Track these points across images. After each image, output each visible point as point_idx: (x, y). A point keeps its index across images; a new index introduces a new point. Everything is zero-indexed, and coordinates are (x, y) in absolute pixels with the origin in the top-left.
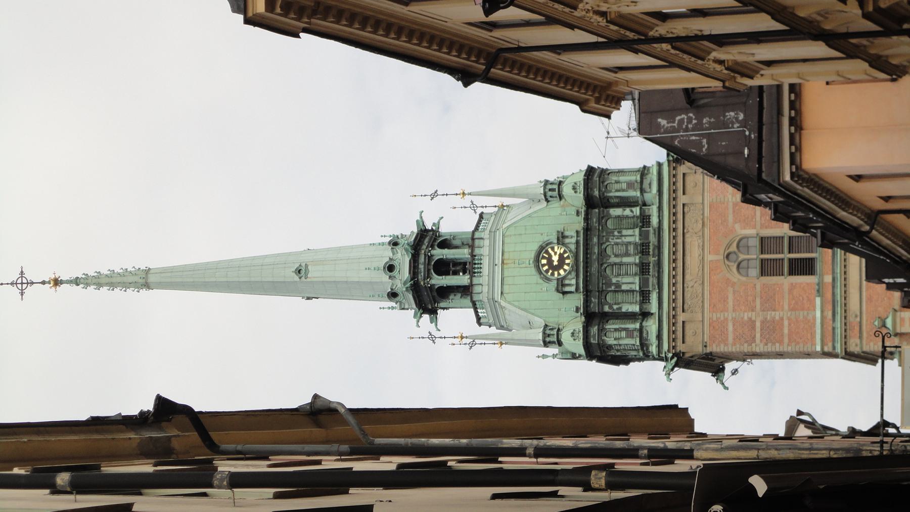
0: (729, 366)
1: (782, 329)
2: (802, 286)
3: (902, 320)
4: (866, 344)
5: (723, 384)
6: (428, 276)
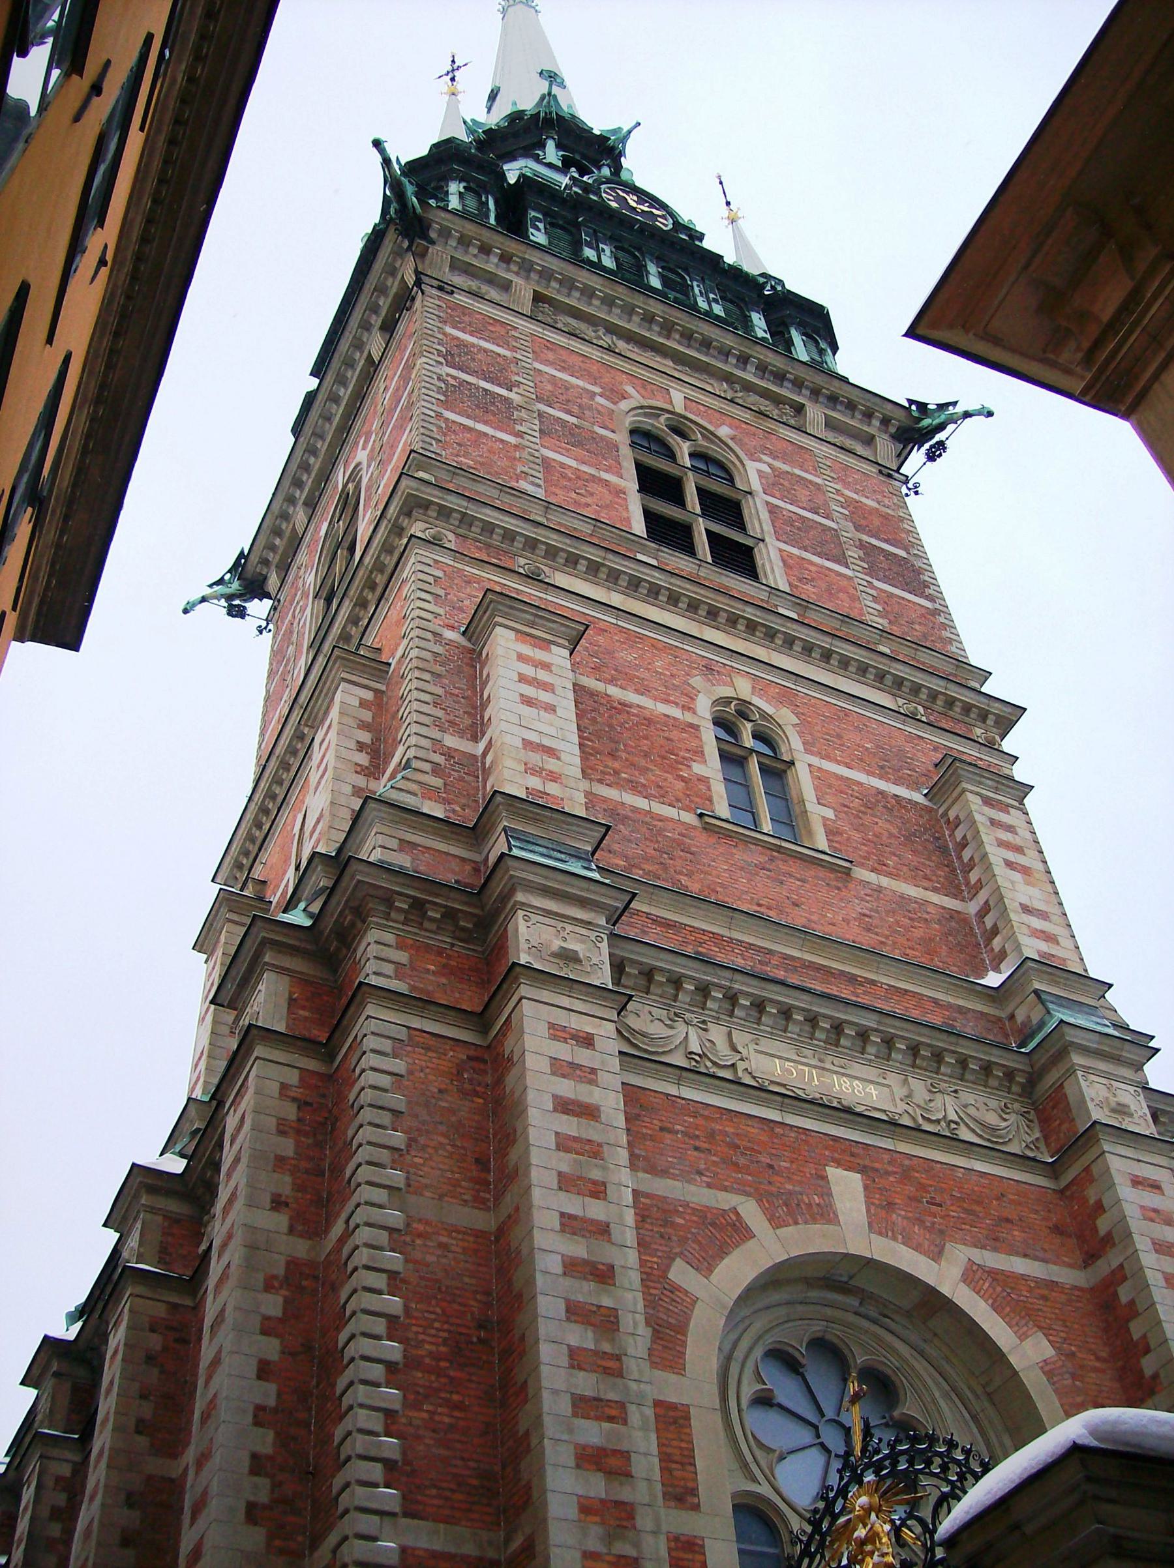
0: (259, 608)
1: (486, 423)
2: (620, 509)
3: (545, 644)
4: (436, 561)
5: (204, 600)
6: (559, 146)
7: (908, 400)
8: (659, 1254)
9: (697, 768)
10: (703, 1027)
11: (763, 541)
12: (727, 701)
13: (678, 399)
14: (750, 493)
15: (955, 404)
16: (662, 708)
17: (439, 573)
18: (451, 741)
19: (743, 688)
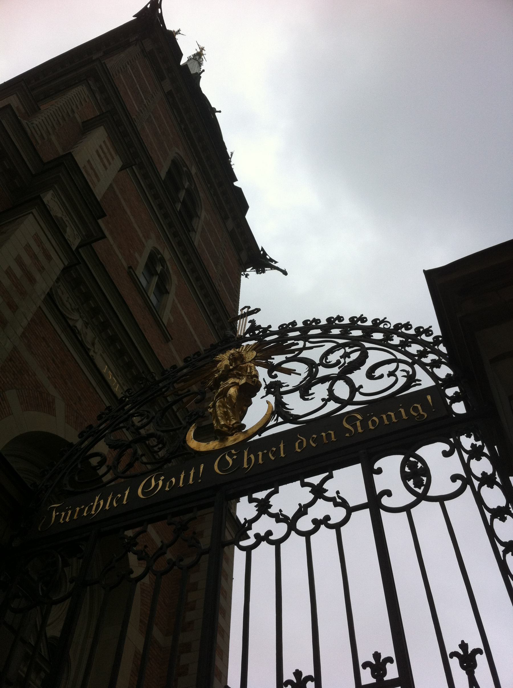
7: (262, 248)
8: (7, 379)
9: (137, 255)
10: (86, 324)
11: (196, 232)
12: (159, 253)
13: (194, 170)
14: (199, 218)
15: (276, 262)
16: (135, 226)
17: (87, 100)
18: (53, 138)
19: (167, 255)
